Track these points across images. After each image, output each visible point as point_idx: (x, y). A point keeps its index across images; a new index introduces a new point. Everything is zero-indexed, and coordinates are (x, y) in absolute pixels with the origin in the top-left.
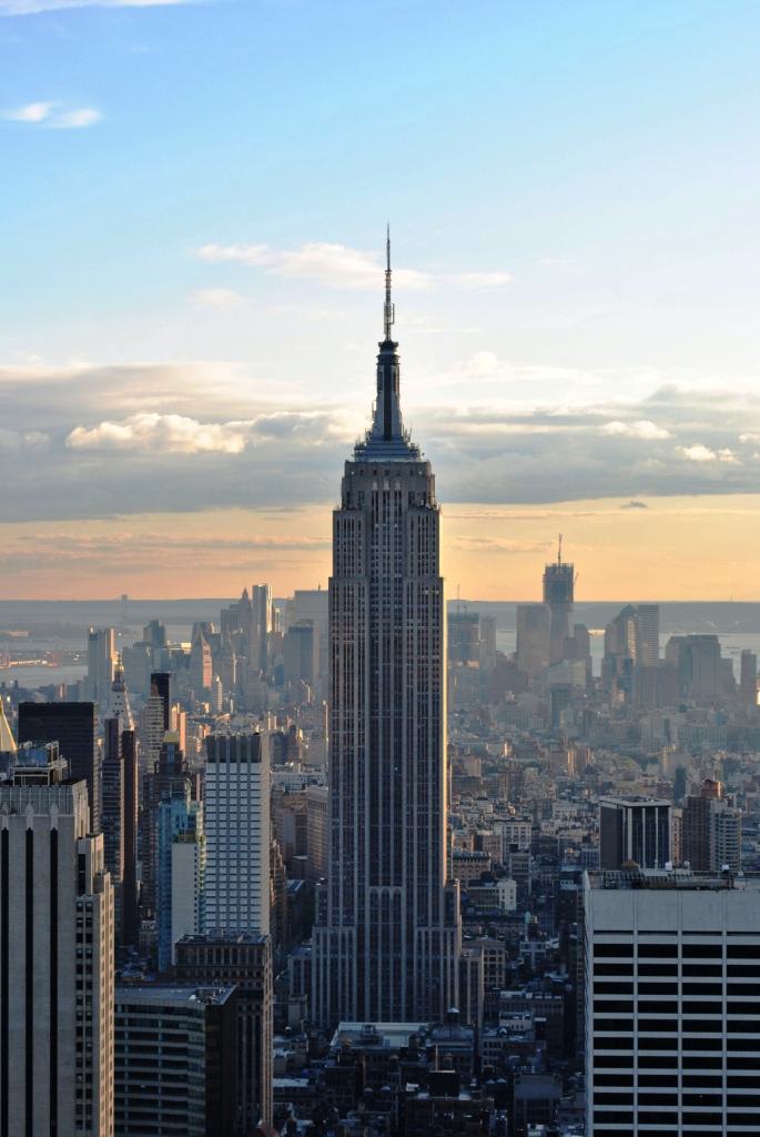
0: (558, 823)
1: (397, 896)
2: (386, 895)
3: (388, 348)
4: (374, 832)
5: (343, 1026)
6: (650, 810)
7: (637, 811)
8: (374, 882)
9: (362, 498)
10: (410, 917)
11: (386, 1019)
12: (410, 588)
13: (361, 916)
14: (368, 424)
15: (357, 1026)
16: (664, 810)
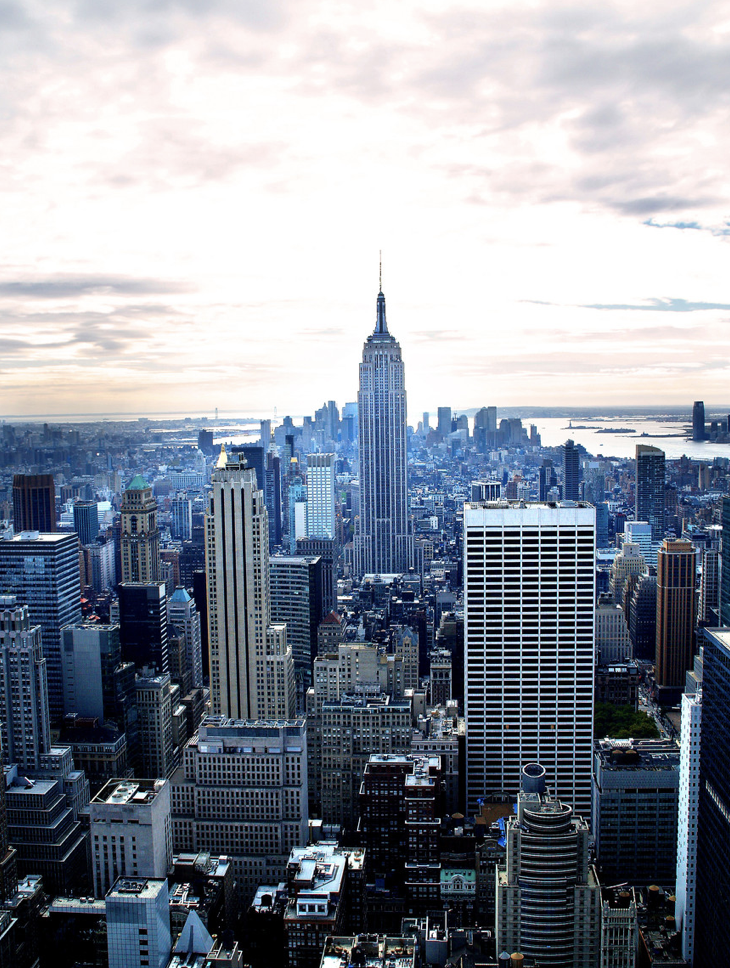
0: (455, 495)
1: (388, 522)
2: (383, 522)
3: (381, 294)
4: (378, 497)
5: (366, 575)
6: (492, 486)
7: (487, 487)
8: (378, 517)
9: (371, 357)
10: (393, 531)
11: (384, 572)
12: (392, 395)
13: (373, 531)
14: (370, 328)
15: (372, 575)
16: (498, 486)
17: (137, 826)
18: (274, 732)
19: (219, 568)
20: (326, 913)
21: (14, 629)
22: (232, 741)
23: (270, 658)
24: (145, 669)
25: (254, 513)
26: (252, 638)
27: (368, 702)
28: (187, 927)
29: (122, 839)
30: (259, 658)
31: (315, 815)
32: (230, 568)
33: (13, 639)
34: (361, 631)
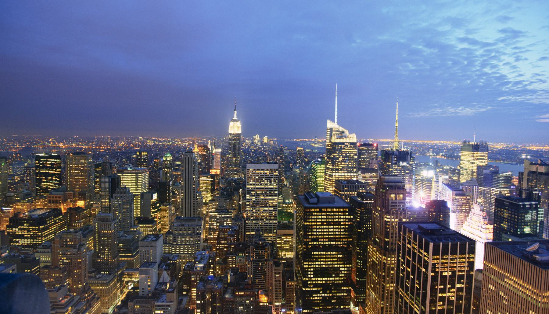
17: (152, 247)
18: (194, 220)
19: (184, 177)
20: (202, 269)
21: (125, 194)
22: (183, 223)
23: (197, 201)
24: (165, 203)
25: (194, 163)
26: (192, 195)
27: (222, 212)
28: (162, 276)
29: (148, 251)
30: (194, 200)
31: (207, 242)
32: (187, 178)
33: (125, 196)
34: (225, 193)
